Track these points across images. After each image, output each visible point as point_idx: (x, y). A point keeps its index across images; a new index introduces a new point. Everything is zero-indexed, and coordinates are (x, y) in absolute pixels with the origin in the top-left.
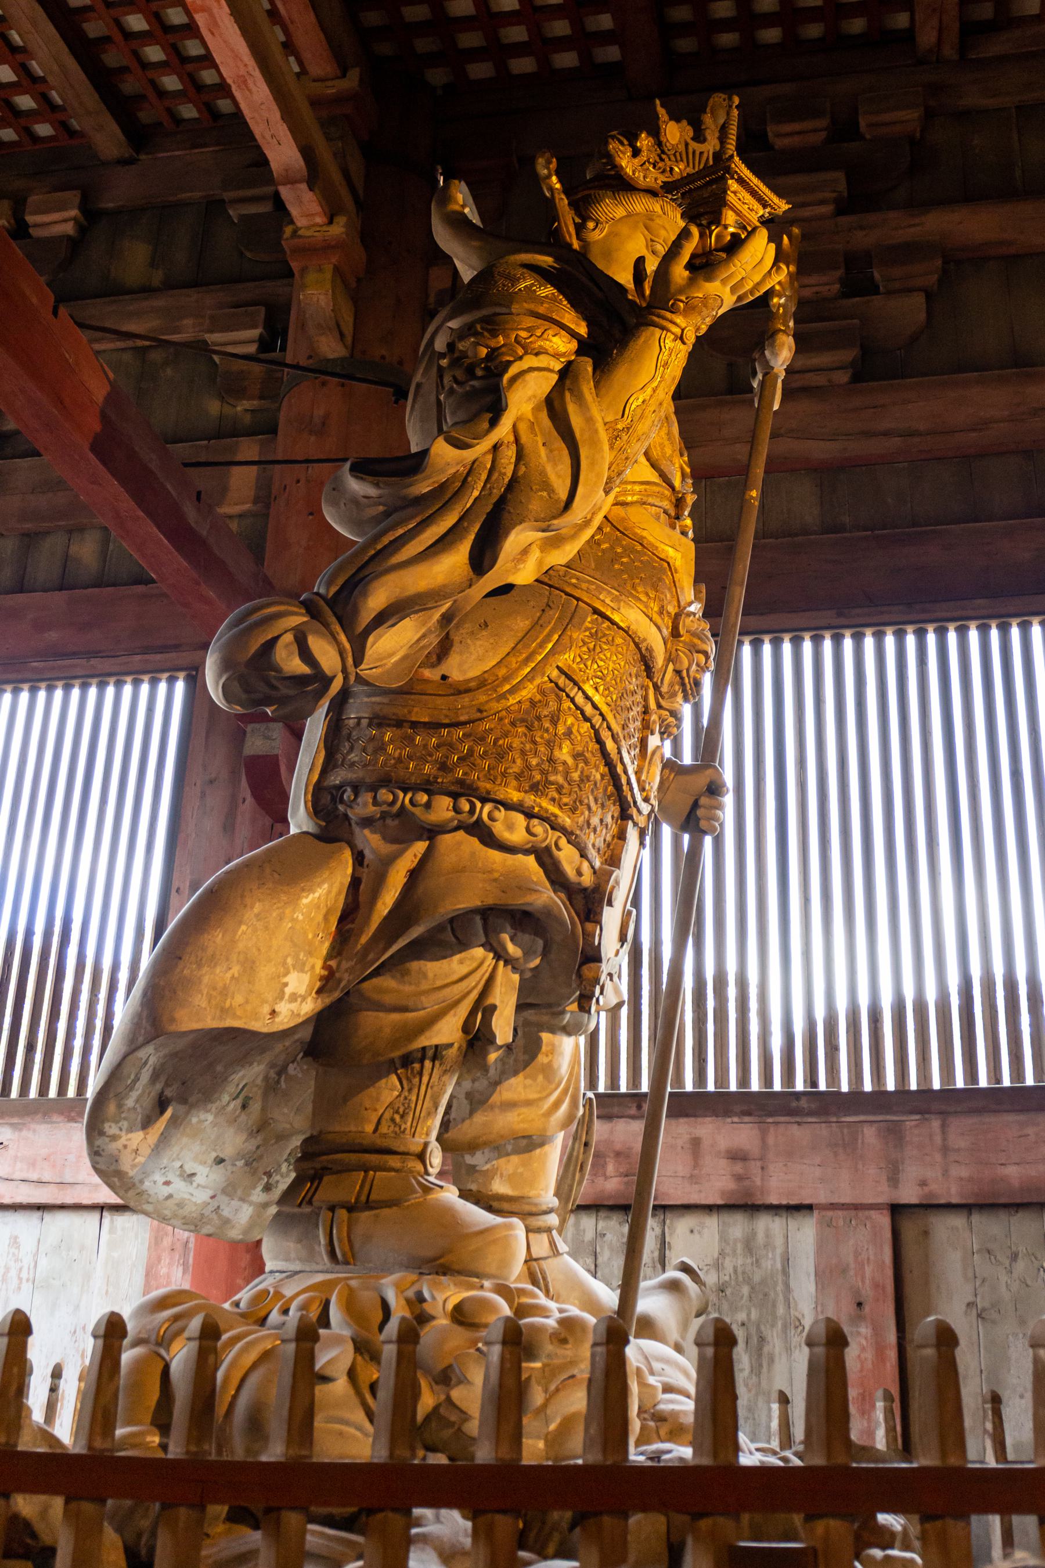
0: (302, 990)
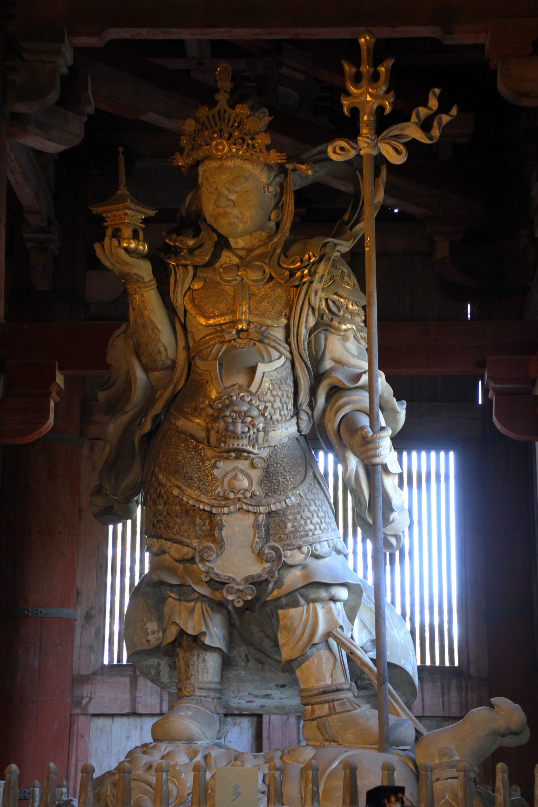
0: (156, 628)
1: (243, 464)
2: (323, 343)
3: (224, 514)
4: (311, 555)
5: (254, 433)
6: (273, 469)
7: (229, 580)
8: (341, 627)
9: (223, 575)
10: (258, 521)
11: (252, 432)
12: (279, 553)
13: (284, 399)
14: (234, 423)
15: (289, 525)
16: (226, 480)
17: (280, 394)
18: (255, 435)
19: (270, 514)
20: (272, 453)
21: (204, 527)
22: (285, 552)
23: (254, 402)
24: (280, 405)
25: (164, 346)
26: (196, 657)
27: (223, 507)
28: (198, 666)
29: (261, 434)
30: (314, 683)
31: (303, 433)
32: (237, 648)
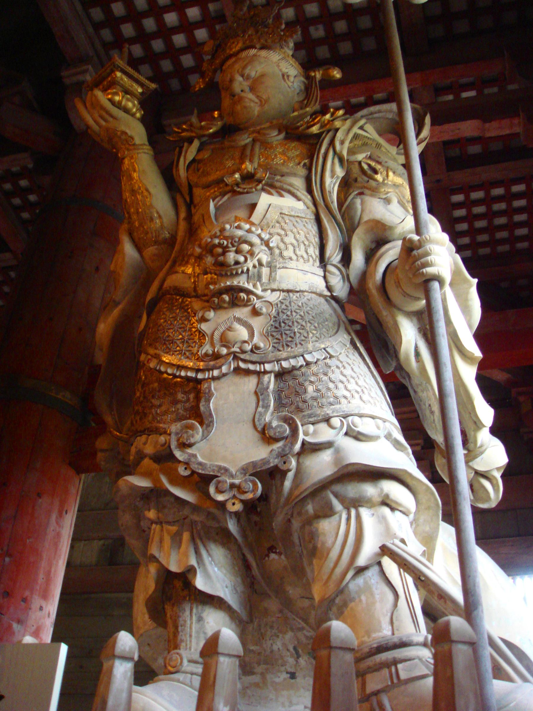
1: (242, 312)
2: (359, 207)
3: (214, 379)
4: (346, 434)
5: (254, 267)
6: (285, 317)
7: (219, 472)
8: (403, 541)
9: (211, 465)
10: (262, 383)
11: (250, 264)
12: (294, 425)
13: (302, 238)
14: (224, 253)
15: (310, 389)
16: (217, 336)
17: (295, 230)
18: (256, 270)
19: (280, 375)
20: (284, 299)
21: (188, 404)
22: (305, 427)
23: (253, 229)
24: (294, 242)
25: (158, 213)
26: (188, 613)
27: (212, 370)
28: (191, 628)
29: (265, 271)
30: (363, 637)
31: (335, 294)
32: (281, 636)
